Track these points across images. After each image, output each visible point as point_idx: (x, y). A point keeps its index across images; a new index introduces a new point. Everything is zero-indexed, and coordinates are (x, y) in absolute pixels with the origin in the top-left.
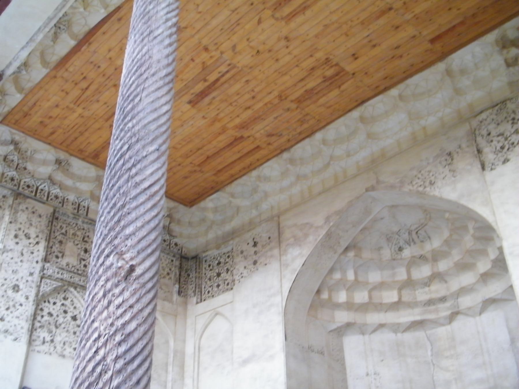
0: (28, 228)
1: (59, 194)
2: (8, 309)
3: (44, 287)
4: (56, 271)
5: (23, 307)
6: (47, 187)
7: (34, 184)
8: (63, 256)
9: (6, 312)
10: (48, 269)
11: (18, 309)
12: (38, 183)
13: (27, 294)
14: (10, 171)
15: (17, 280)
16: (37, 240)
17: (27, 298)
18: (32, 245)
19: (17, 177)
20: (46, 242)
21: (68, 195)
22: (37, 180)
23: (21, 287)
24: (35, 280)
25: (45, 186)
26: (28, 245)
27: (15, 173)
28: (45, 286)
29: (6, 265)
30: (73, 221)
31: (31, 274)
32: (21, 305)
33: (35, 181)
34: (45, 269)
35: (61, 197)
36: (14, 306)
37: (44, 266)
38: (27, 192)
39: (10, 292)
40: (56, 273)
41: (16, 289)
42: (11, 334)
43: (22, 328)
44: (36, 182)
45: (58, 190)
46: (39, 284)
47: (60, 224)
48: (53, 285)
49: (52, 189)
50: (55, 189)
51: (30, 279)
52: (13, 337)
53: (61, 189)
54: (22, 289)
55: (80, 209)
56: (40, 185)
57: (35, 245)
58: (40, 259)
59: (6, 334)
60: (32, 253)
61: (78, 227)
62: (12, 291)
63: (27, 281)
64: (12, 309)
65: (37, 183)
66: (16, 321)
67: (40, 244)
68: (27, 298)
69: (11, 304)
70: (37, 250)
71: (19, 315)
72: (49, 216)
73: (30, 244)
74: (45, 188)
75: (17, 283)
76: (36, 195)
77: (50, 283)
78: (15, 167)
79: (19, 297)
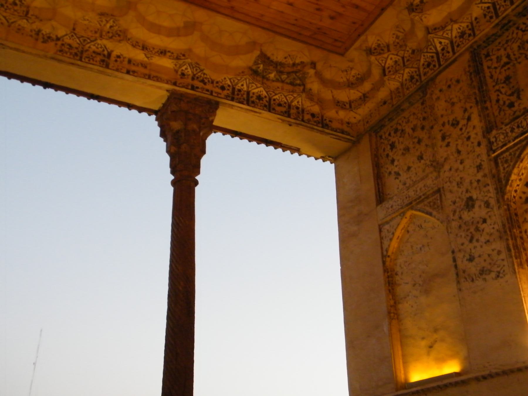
0: (452, 112)
1: (461, 28)
2: (471, 241)
3: (504, 169)
4: (508, 130)
5: (489, 221)
6: (443, 41)
7: (431, 54)
8: (519, 98)
9: (471, 246)
10: (496, 141)
11: (483, 231)
12: (431, 49)
13: (486, 199)
14: (403, 74)
15: (467, 191)
16: (467, 115)
17: (487, 204)
18: (464, 128)
19: (413, 70)
20: (478, 106)
21: (471, 14)
22: (427, 49)
23: (475, 197)
24: (487, 171)
25: (440, 43)
26: (460, 133)
27: (407, 70)
28: (506, 165)
29: (448, 184)
30: (511, 31)
31: (479, 167)
32: (485, 221)
33: (427, 52)
34: (493, 143)
35: (468, 26)
36: (477, 229)
37: (489, 140)
38: (431, 73)
39: (467, 216)
40: (510, 134)
41: (470, 203)
42: (490, 271)
43: (499, 253)
44: (429, 50)
45: (456, 26)
46: (494, 171)
47: (494, 58)
48: (515, 154)
49: (450, 34)
50: (452, 30)
51: (479, 176)
52: (493, 275)
53: (456, 22)
54: (477, 199)
55: (498, 7)
56: (436, 48)
57: (467, 124)
58: (480, 137)
59: (484, 276)
60: (468, 138)
61: (521, 30)
62: (467, 210)
63: (478, 181)
64: (477, 236)
65: (431, 51)
66: (487, 249)
67: (472, 119)
68: (487, 204)
69: (472, 230)
70: (472, 127)
71: (488, 238)
72: (467, 69)
73: (461, 129)
74: (443, 44)
75: (468, 195)
76: (440, 65)
77: (510, 154)
78: (402, 65)
79: (479, 212)
